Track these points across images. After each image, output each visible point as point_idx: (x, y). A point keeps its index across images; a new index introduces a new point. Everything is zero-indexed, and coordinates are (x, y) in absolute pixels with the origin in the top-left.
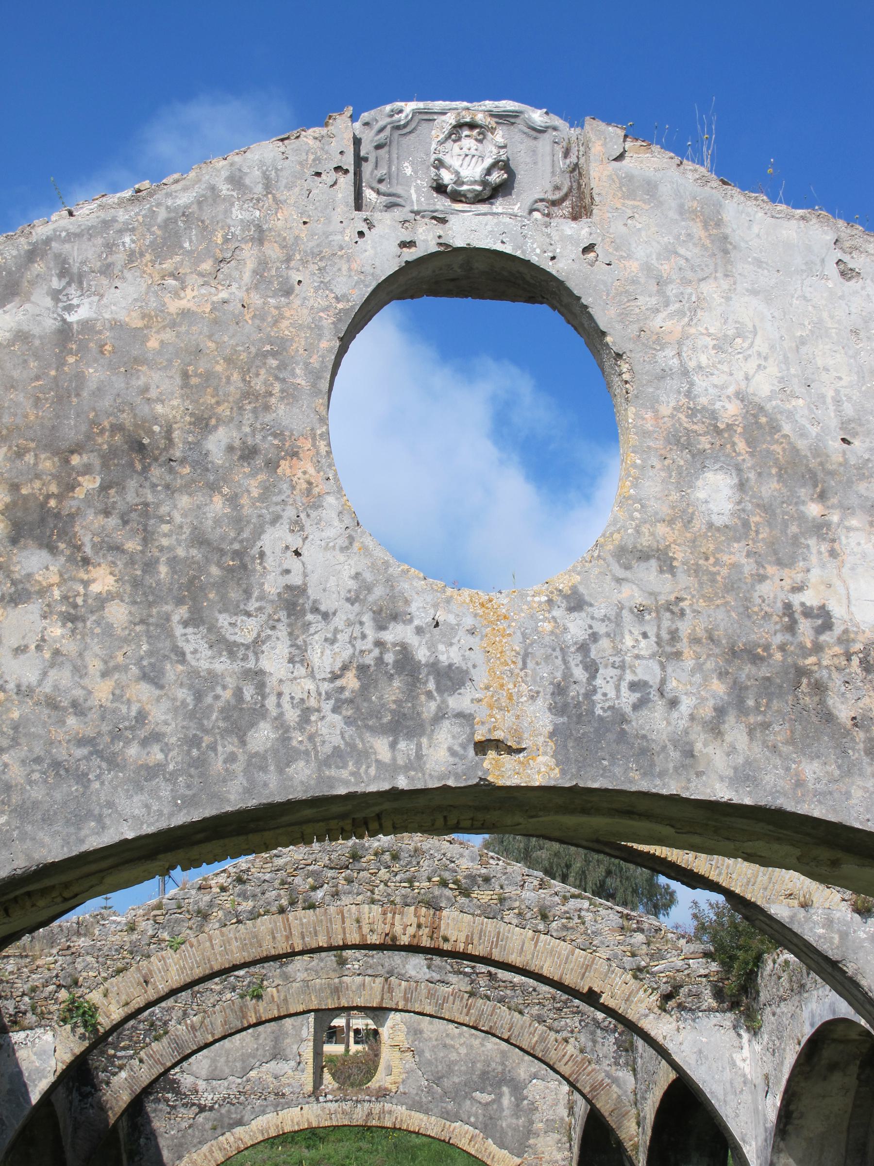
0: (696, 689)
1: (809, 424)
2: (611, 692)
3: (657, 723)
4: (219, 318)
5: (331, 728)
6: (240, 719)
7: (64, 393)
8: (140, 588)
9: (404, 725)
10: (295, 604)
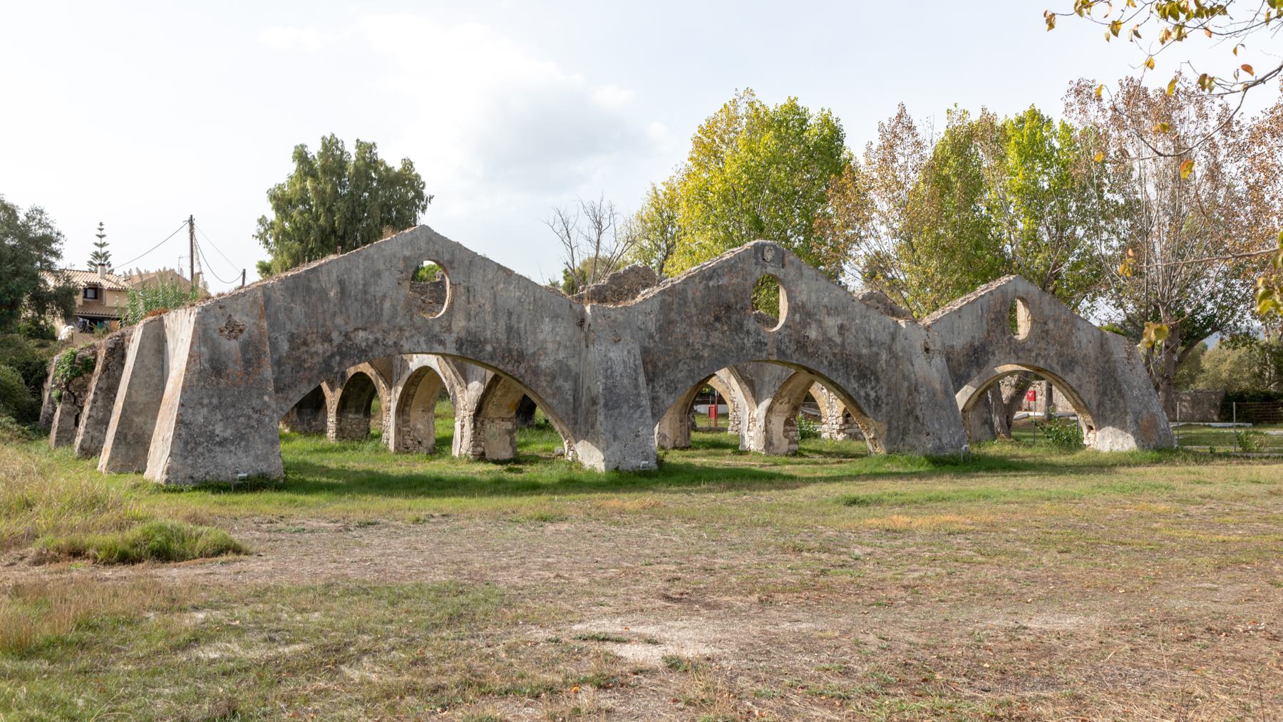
0: (793, 347)
1: (809, 306)
2: (783, 347)
3: (788, 352)
4: (738, 285)
5: (752, 351)
6: (742, 349)
7: (719, 296)
8: (729, 329)
9: (760, 351)
10: (748, 332)
